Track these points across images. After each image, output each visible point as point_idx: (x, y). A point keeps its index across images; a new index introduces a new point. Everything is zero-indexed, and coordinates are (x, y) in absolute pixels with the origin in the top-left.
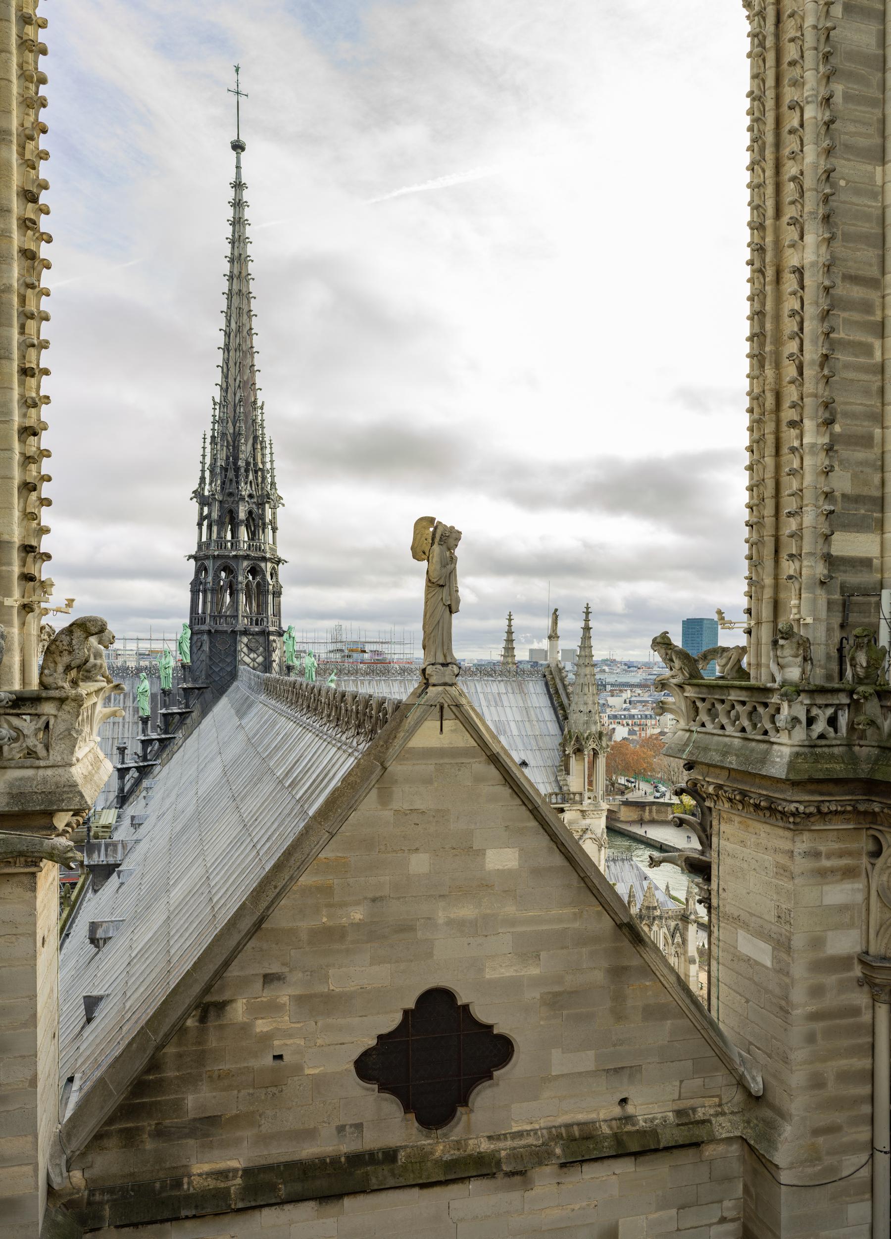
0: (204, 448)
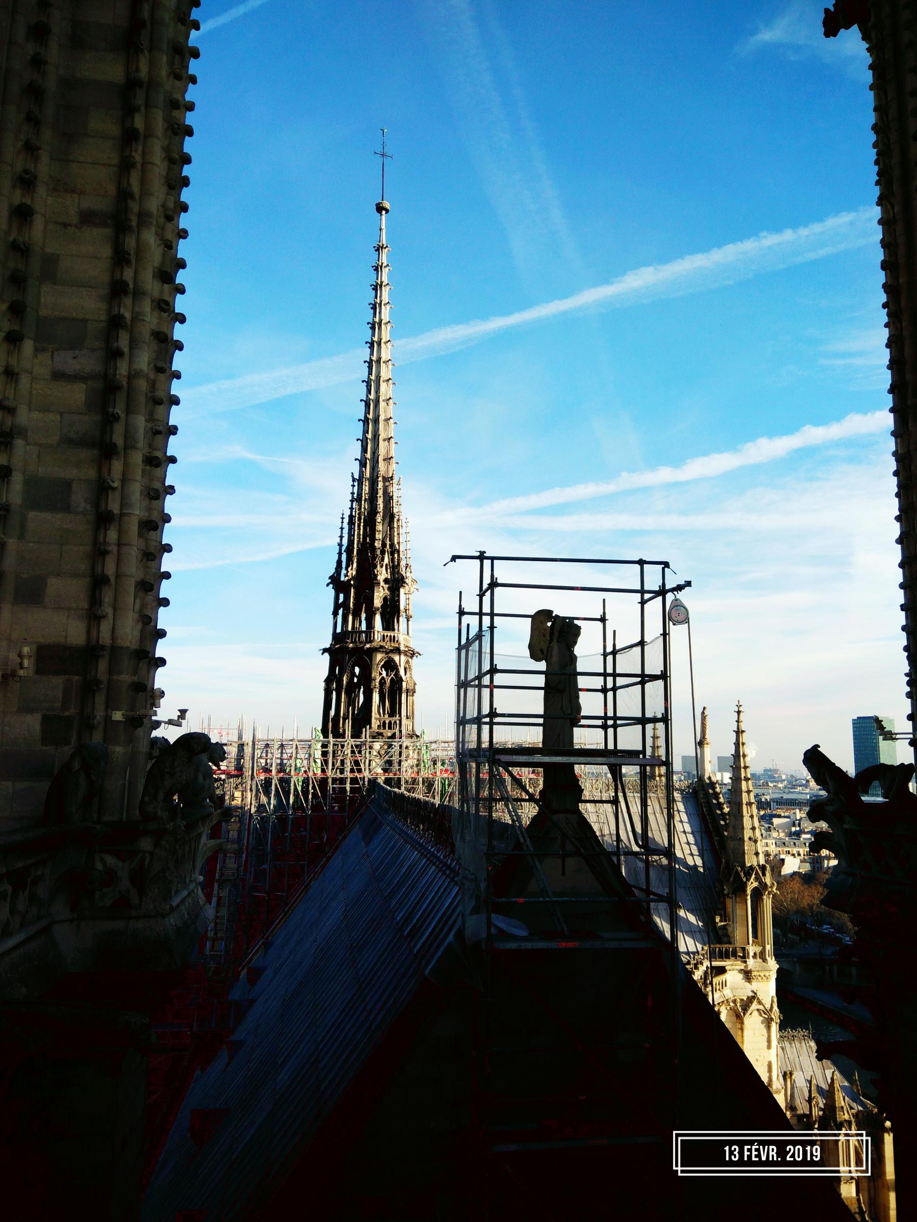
0: (342, 528)
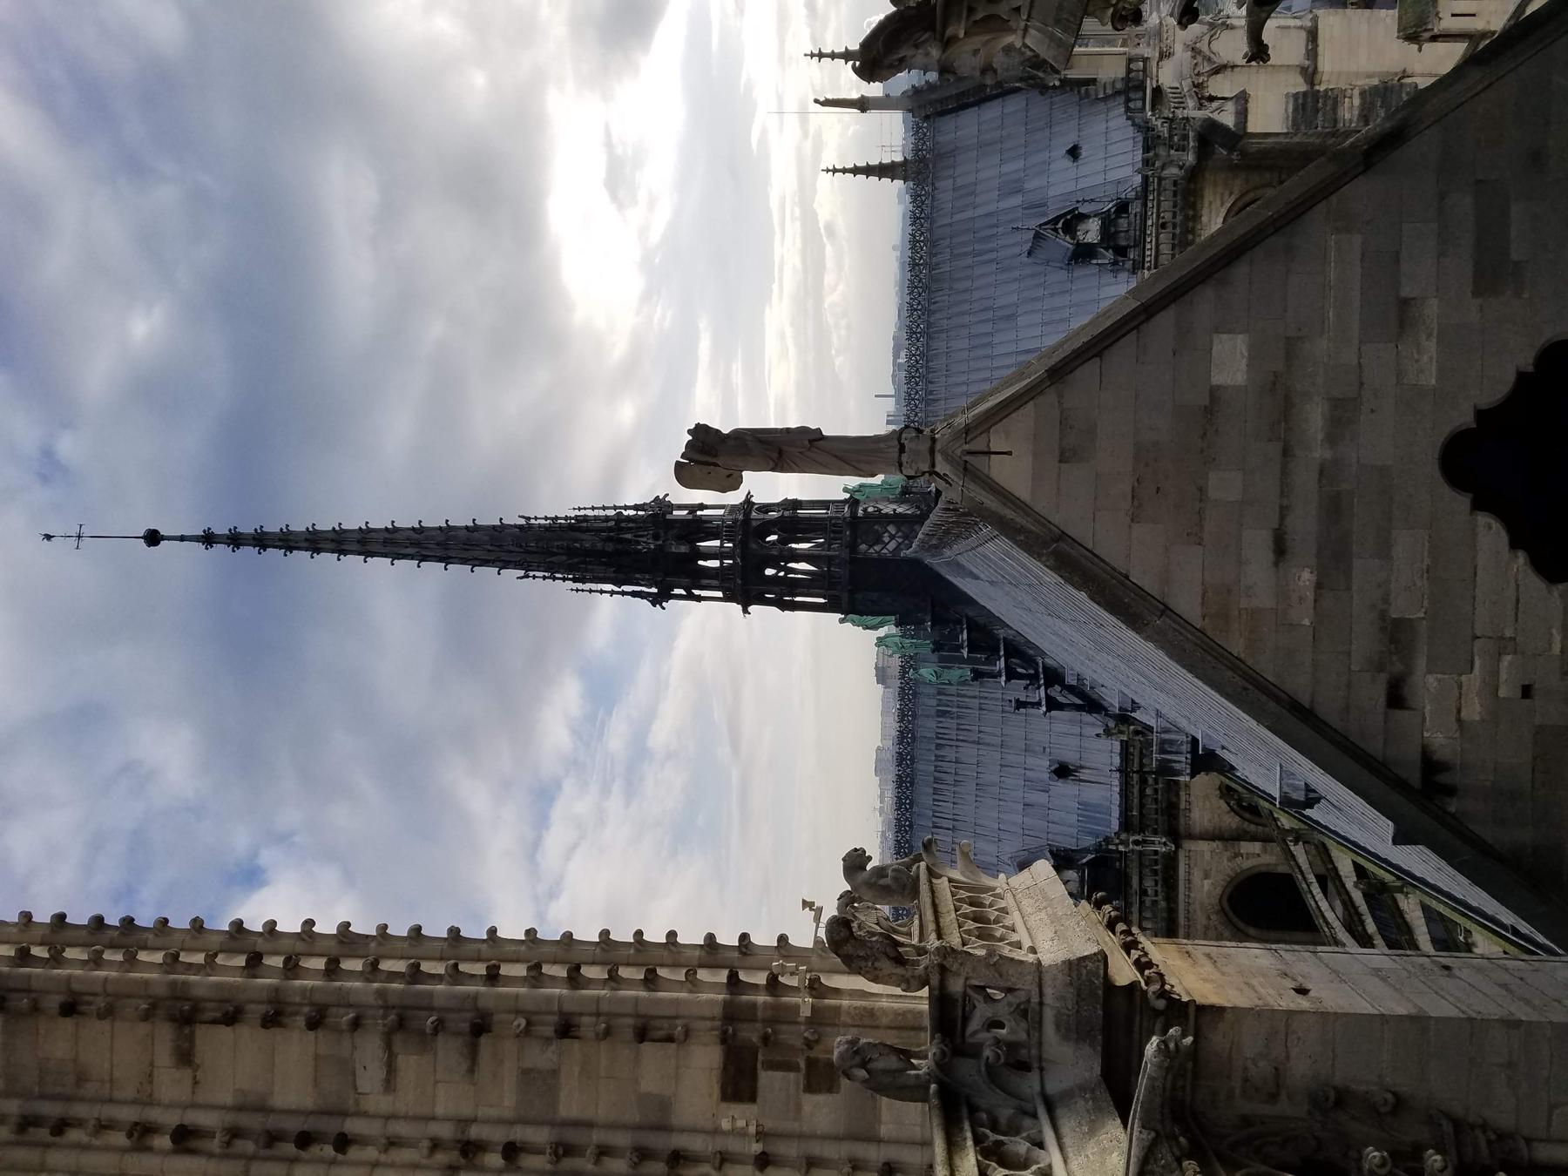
0: (591, 591)
